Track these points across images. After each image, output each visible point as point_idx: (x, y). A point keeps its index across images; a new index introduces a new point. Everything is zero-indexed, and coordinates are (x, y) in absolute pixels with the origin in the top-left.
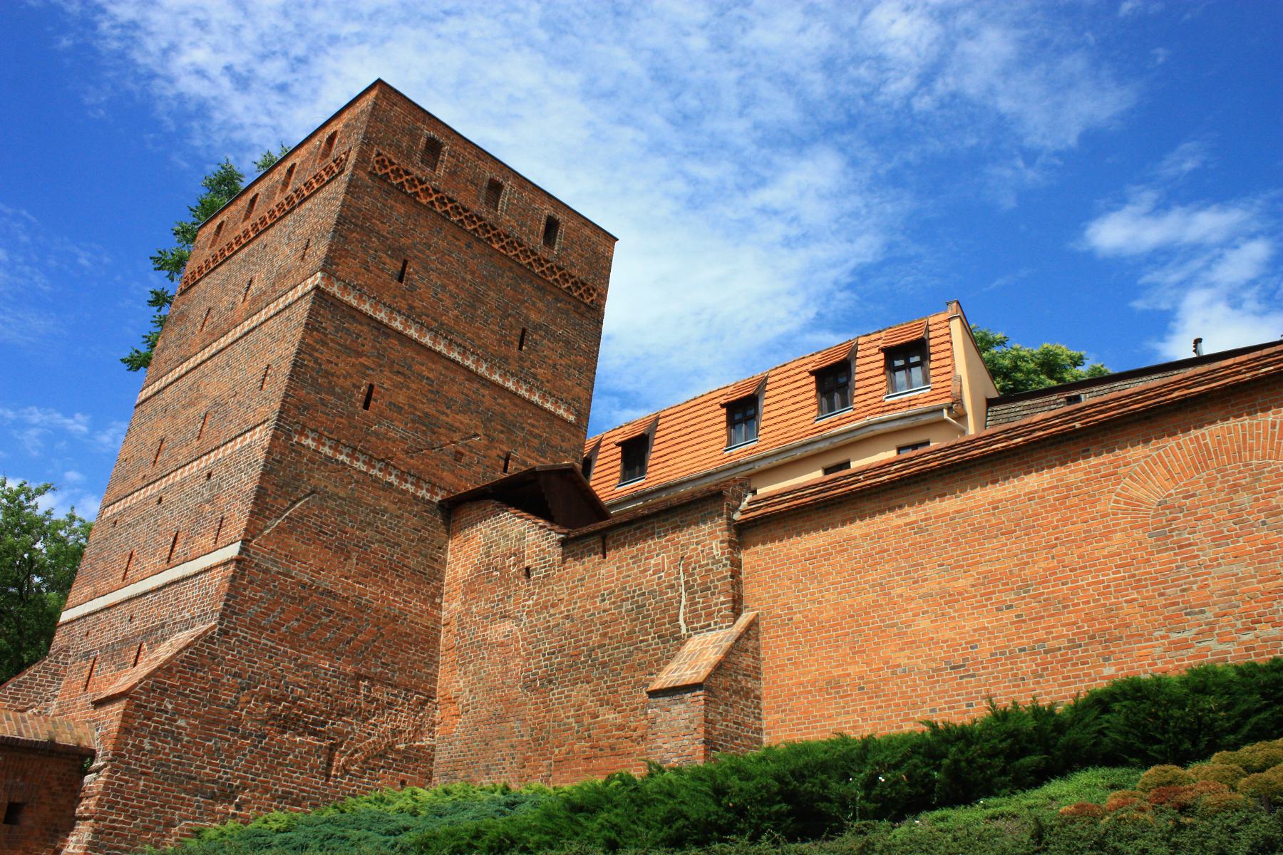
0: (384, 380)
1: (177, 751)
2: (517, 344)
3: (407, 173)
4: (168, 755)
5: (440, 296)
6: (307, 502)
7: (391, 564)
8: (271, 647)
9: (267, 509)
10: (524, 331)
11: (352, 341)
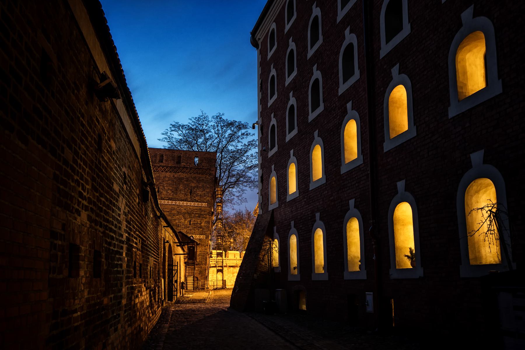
2: (190, 194)
5: (168, 192)
10: (191, 190)
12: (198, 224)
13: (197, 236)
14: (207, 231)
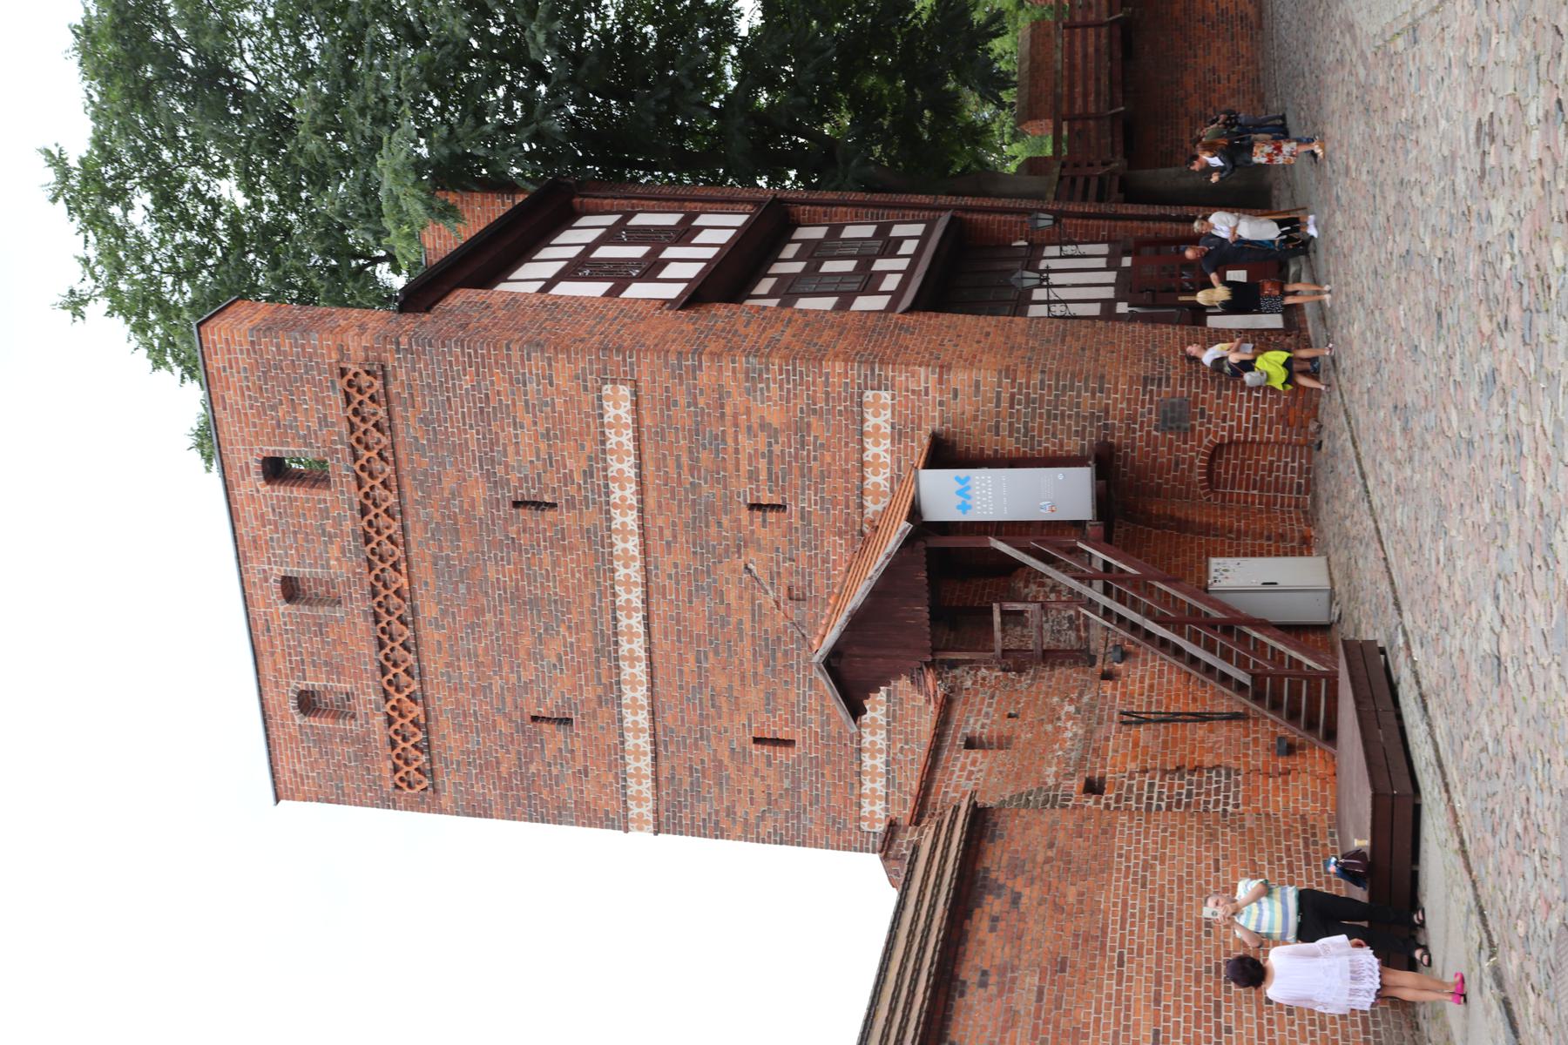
2: (549, 515)
5: (554, 660)
10: (516, 504)
11: (704, 777)
12: (777, 449)
13: (876, 456)
14: (826, 384)
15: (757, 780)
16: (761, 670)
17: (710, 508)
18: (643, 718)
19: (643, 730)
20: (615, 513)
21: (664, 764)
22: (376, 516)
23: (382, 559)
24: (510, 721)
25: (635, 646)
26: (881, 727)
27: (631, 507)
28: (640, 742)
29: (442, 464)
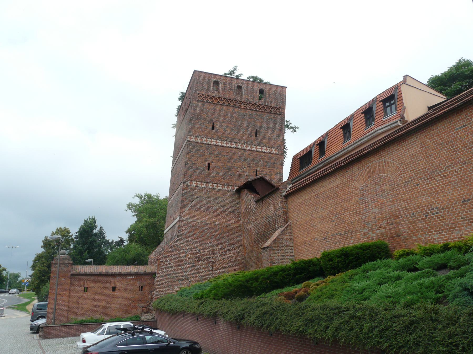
0: (211, 161)
1: (172, 270)
2: (255, 135)
3: (208, 96)
4: (170, 272)
5: (226, 129)
6: (196, 201)
7: (223, 211)
8: (192, 241)
9: (185, 205)
10: (256, 130)
11: (201, 152)
15: (200, 162)
16: (224, 166)
17: (257, 163)
18: (214, 143)
19: (211, 143)
20: (255, 147)
21: (204, 145)
22: (254, 106)
23: (246, 104)
24: (213, 119)
25: (229, 145)
26: (212, 187)
27: (256, 149)
28: (209, 142)
29: (264, 119)
